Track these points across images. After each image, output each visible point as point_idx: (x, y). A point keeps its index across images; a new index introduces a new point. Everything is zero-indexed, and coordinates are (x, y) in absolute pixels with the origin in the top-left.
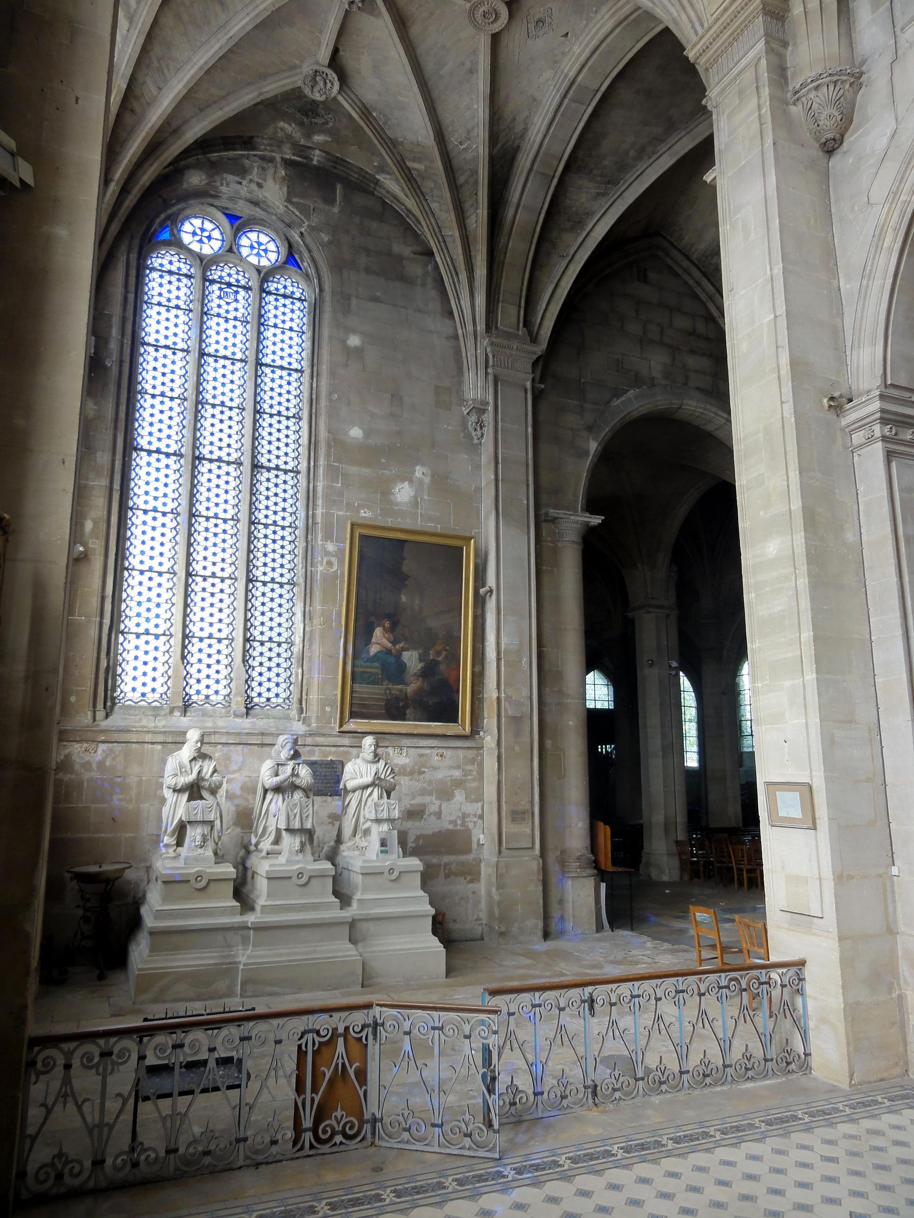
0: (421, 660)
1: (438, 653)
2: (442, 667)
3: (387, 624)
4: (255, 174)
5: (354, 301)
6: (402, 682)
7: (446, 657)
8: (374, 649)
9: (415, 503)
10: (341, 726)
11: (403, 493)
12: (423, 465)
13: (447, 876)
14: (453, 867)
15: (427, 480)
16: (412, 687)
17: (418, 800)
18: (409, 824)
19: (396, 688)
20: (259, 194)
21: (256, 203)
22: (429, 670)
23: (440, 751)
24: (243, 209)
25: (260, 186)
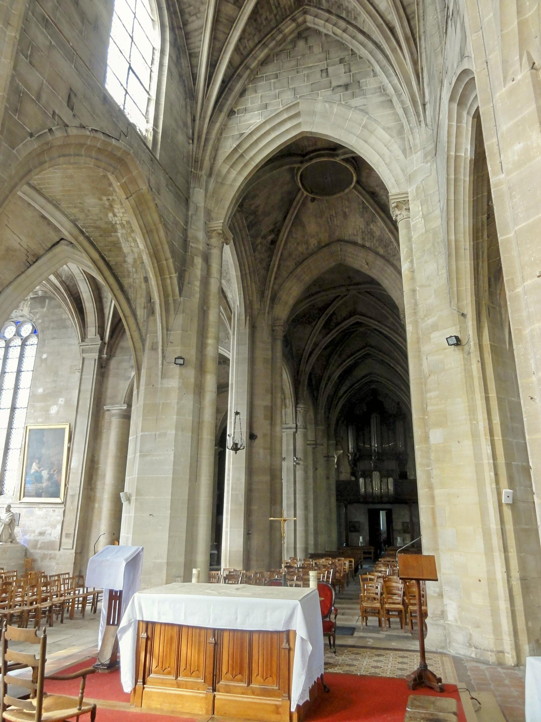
0: (48, 474)
1: (54, 471)
2: (55, 476)
3: (37, 461)
4: (21, 308)
5: (46, 342)
6: (41, 483)
7: (57, 472)
8: (33, 471)
9: (58, 413)
10: (20, 500)
11: (54, 410)
12: (62, 397)
13: (50, 559)
14: (52, 555)
15: (63, 403)
16: (44, 485)
17: (44, 528)
18: (39, 538)
19: (39, 485)
20: (21, 313)
21: (22, 316)
22: (50, 478)
23: (54, 509)
24: (21, 319)
25: (22, 310)
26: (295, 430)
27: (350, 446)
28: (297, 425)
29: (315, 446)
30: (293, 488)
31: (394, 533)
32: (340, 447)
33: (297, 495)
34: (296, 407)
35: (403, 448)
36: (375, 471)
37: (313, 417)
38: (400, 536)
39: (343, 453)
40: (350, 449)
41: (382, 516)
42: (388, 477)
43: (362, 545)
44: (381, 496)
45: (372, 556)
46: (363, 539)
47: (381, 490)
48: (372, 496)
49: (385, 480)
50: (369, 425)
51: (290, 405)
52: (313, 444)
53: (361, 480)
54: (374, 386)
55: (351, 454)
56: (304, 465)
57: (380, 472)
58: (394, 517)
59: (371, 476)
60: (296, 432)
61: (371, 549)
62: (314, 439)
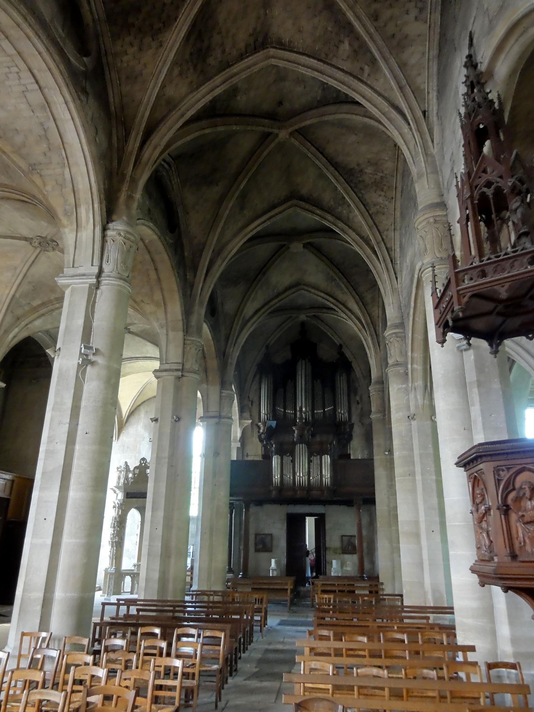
26: (94, 281)
27: (263, 412)
28: (101, 271)
29: (180, 373)
30: (65, 428)
31: (327, 552)
32: (246, 414)
33: (77, 447)
34: (104, 229)
35: (347, 415)
36: (301, 443)
37: (180, 317)
38: (335, 559)
39: (252, 423)
40: (262, 415)
41: (310, 523)
42: (321, 453)
43: (275, 574)
44: (309, 488)
45: (288, 597)
46: (276, 562)
47: (309, 476)
48: (293, 487)
49: (316, 460)
50: (293, 378)
51: (88, 221)
52: (177, 370)
53: (275, 461)
54: (303, 317)
55: (265, 423)
56: (108, 368)
57: (309, 445)
58: (328, 526)
59: (292, 454)
60: (98, 285)
61: (286, 584)
62: (180, 361)
